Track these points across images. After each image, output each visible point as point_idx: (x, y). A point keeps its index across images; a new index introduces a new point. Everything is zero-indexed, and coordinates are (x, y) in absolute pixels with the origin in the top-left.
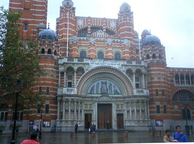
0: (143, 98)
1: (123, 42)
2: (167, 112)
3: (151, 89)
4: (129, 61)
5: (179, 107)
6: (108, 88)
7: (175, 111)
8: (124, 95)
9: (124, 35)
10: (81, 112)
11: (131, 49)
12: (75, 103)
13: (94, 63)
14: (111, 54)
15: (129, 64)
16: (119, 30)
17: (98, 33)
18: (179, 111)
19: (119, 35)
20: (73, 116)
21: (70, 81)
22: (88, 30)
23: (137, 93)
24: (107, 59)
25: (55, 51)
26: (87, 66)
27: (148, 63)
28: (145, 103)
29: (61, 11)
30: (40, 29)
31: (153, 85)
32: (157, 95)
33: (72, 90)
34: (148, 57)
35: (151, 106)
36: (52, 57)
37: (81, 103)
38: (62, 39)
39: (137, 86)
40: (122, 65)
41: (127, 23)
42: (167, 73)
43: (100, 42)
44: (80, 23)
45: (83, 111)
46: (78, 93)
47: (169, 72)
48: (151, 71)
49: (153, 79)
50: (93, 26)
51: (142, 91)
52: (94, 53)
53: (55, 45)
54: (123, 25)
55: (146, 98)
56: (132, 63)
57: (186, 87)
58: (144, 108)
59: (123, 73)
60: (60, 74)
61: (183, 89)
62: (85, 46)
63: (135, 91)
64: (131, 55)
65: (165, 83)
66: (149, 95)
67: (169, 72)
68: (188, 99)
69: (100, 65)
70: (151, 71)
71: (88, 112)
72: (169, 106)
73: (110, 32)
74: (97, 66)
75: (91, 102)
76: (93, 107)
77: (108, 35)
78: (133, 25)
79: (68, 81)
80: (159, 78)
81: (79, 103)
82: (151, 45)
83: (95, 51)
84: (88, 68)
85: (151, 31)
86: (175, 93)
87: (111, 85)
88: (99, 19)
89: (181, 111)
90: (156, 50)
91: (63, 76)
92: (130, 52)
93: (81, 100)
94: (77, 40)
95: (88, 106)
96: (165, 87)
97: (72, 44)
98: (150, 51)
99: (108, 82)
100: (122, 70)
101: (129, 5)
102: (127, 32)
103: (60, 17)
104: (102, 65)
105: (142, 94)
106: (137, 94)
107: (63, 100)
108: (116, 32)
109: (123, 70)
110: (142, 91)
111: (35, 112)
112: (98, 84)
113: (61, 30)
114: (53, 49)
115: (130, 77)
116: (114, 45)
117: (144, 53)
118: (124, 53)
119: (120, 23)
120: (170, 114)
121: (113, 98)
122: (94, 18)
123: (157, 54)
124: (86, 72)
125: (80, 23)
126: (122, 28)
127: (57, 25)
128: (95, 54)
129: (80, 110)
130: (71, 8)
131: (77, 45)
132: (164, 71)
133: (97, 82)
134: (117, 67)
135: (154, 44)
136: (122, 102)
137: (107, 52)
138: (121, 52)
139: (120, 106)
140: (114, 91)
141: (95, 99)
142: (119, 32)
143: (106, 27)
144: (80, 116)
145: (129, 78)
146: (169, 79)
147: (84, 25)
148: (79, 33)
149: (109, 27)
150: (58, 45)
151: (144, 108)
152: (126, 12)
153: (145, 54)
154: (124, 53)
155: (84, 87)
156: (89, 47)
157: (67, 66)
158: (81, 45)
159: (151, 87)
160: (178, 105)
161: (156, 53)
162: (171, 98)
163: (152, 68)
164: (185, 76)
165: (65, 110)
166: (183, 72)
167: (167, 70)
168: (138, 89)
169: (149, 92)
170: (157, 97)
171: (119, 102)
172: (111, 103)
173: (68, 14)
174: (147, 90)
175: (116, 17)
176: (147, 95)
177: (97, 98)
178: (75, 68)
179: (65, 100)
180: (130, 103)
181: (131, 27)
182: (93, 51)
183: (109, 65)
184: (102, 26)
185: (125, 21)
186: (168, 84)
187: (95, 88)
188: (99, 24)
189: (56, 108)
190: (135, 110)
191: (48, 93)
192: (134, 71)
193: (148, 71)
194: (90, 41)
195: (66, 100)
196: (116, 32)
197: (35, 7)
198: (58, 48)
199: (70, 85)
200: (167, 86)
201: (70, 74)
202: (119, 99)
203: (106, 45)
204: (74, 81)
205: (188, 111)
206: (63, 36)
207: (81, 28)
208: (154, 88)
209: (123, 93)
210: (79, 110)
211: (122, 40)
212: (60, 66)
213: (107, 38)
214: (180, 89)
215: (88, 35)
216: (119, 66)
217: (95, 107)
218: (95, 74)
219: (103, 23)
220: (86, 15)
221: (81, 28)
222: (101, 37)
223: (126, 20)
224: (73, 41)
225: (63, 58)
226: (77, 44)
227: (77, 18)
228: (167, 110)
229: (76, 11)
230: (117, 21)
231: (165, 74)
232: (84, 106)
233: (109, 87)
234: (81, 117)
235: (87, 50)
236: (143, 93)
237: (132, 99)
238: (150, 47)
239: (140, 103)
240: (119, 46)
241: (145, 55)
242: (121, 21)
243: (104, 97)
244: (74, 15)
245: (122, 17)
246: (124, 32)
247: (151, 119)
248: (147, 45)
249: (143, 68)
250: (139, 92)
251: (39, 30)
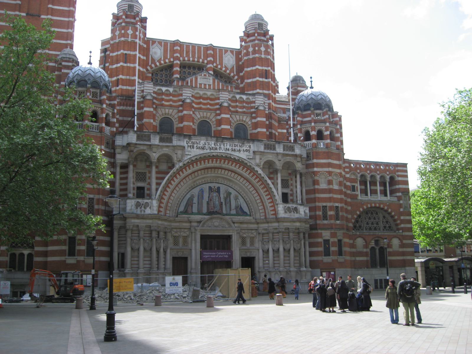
0: (298, 224)
1: (254, 102)
2: (343, 254)
3: (313, 205)
4: (268, 145)
5: (366, 242)
6: (222, 200)
7: (358, 250)
8: (258, 216)
9: (254, 86)
10: (165, 252)
11: (269, 117)
12: (154, 234)
13: (195, 145)
14: (228, 127)
15: (269, 151)
16: (241, 74)
17: (199, 80)
18: (365, 250)
19: (241, 86)
20: (147, 262)
21: (140, 184)
22: (175, 69)
23: (286, 212)
24: (219, 137)
25: (107, 115)
26: (179, 152)
27: (307, 148)
28: (302, 235)
29: (113, 24)
30: (63, 63)
31: (317, 195)
32: (325, 217)
33: (146, 205)
34: (308, 137)
35: (312, 240)
36: (101, 130)
37: (165, 233)
38: (118, 88)
39: (285, 198)
40: (254, 152)
41: (260, 59)
42: (344, 171)
43: (204, 99)
44: (157, 52)
45: (168, 251)
46: (159, 211)
47: (347, 170)
48: (313, 165)
49: (318, 184)
50: (184, 60)
51: (296, 210)
52: (191, 124)
53: (107, 102)
54: (253, 62)
55: (304, 224)
56: (274, 149)
57: (381, 202)
58: (299, 245)
59: (257, 169)
60: (118, 170)
61: (373, 205)
62: (171, 106)
63: (281, 208)
64: (270, 130)
65: (340, 192)
66: (308, 217)
67: (347, 170)
68: (381, 225)
69: (208, 151)
70: (313, 165)
71: (180, 255)
72: (346, 240)
73: (221, 77)
74: (202, 152)
75: (186, 230)
76: (192, 243)
77: (221, 84)
78: (274, 64)
79: (136, 184)
80: (330, 182)
81: (162, 234)
82: (314, 109)
83: (193, 118)
84: (183, 156)
85: (312, 79)
86: (358, 213)
87: (229, 194)
88: (199, 46)
89: (368, 250)
90: (324, 121)
91: (127, 173)
92: (267, 123)
93: (166, 228)
94: (154, 92)
95: (181, 240)
96: (341, 201)
97: (142, 102)
98: (313, 124)
99: (223, 189)
100: (253, 163)
101: (265, 19)
102: (261, 79)
103: (112, 38)
104: (212, 151)
105: (296, 216)
106: (287, 215)
107: (128, 227)
108: (236, 77)
109: (257, 163)
110: (296, 210)
111: (61, 253)
112: (202, 191)
113: (114, 66)
114: (102, 113)
115: (270, 178)
116: (233, 107)
117: (299, 126)
118: (256, 125)
119: (246, 58)
120: (348, 258)
121: (234, 223)
122: (188, 45)
123: (326, 130)
124: (177, 166)
125: (157, 52)
126: (249, 69)
127: (103, 54)
128: (193, 127)
129: (164, 249)
130: (137, 19)
131: (154, 103)
132: (339, 167)
133: (201, 186)
134: (243, 155)
135: (320, 109)
136: (253, 231)
137: (219, 123)
138: (250, 123)
139: (248, 241)
140: (236, 208)
142: (242, 79)
143: (215, 65)
144: (164, 263)
145: (269, 182)
146: (348, 184)
147: (165, 57)
148: (152, 74)
149: (219, 67)
150: (112, 102)
151: (299, 245)
152: (259, 34)
153: (300, 130)
154: (256, 125)
155: (172, 198)
156: (181, 108)
158: (162, 105)
159: (314, 200)
160: (364, 239)
161: (323, 129)
162: (351, 225)
163: (315, 161)
164: (378, 177)
165: (132, 249)
166: (376, 170)
167: (344, 166)
168: (288, 205)
169: (310, 211)
170: (325, 222)
171: (246, 231)
172: (230, 234)
173: (130, 32)
174: (306, 206)
175: (236, 45)
176: (306, 217)
177: (199, 222)
178: (154, 156)
179: (131, 227)
180: (271, 235)
181: (270, 68)
182: (191, 118)
183: (228, 152)
184: (206, 62)
185: (257, 55)
186: (346, 195)
187: (195, 200)
188: (199, 57)
190: (281, 249)
192: (279, 165)
193: (308, 166)
194: (181, 95)
195: (134, 226)
196: (236, 77)
197: (53, 12)
198: (113, 110)
199: (141, 193)
200: (345, 198)
201: (141, 167)
202: (245, 226)
203: (218, 107)
204: (149, 184)
205: (382, 250)
206: (120, 81)
207: (158, 64)
208: (319, 202)
209: (254, 213)
210: (162, 250)
211: (251, 97)
212: (118, 150)
213: (219, 90)
214: (369, 206)
215: (178, 82)
216: (247, 153)
217: (195, 243)
218: (194, 172)
219: (206, 56)
220: (172, 38)
221: (158, 64)
222: (205, 88)
223: (259, 52)
224: (145, 94)
225: (127, 133)
226: (155, 101)
228: (345, 249)
229: (149, 24)
230: (237, 53)
231: (341, 173)
232: (171, 240)
233: (226, 199)
234: (165, 265)
235: (176, 116)
236: (297, 213)
237: (276, 224)
238: (312, 116)
239: (291, 234)
240: (245, 110)
241: (301, 132)
242: (247, 54)
243: (214, 221)
244: (145, 34)
245: (250, 44)
246: (254, 80)
247: (312, 269)
248: (305, 110)
249: (299, 159)
250: (288, 210)
251: (61, 64)
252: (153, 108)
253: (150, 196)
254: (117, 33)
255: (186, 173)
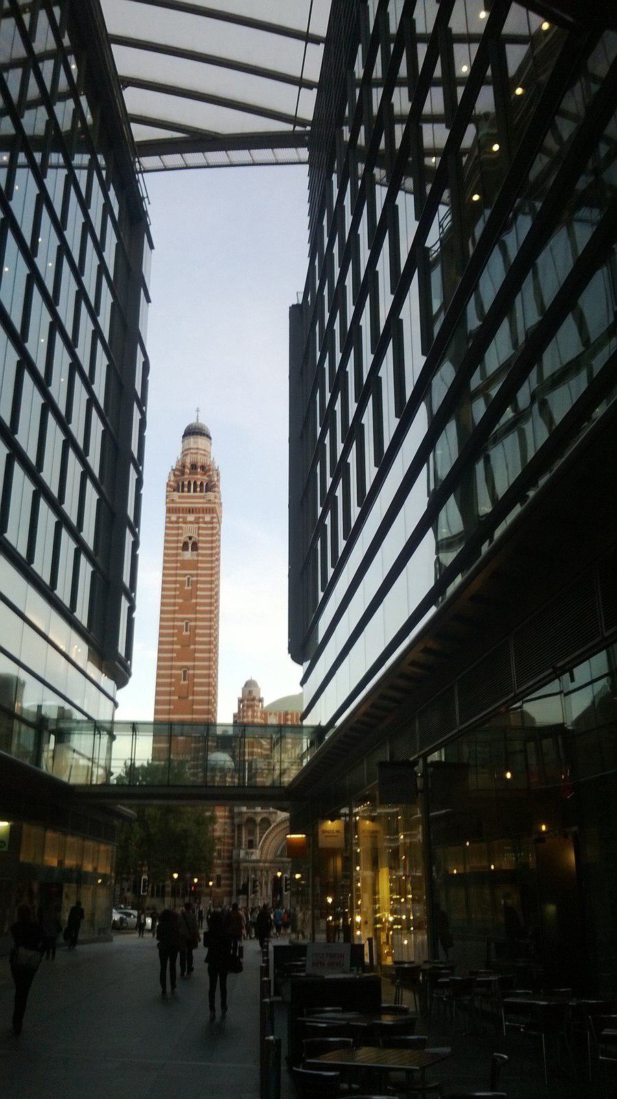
21: (251, 838)
26: (274, 816)
33: (252, 853)
60: (236, 827)
93: (267, 867)
141: (287, 865)
157: (245, 817)
173: (250, 713)
178: (258, 819)
189: (231, 879)
191: (219, 857)
195: (245, 867)
199: (251, 844)
212: (236, 816)
227: (265, 714)
252: (264, 778)
253: (256, 848)
254: (241, 714)
255: (279, 830)
